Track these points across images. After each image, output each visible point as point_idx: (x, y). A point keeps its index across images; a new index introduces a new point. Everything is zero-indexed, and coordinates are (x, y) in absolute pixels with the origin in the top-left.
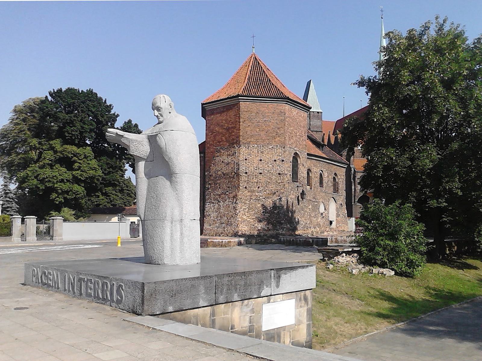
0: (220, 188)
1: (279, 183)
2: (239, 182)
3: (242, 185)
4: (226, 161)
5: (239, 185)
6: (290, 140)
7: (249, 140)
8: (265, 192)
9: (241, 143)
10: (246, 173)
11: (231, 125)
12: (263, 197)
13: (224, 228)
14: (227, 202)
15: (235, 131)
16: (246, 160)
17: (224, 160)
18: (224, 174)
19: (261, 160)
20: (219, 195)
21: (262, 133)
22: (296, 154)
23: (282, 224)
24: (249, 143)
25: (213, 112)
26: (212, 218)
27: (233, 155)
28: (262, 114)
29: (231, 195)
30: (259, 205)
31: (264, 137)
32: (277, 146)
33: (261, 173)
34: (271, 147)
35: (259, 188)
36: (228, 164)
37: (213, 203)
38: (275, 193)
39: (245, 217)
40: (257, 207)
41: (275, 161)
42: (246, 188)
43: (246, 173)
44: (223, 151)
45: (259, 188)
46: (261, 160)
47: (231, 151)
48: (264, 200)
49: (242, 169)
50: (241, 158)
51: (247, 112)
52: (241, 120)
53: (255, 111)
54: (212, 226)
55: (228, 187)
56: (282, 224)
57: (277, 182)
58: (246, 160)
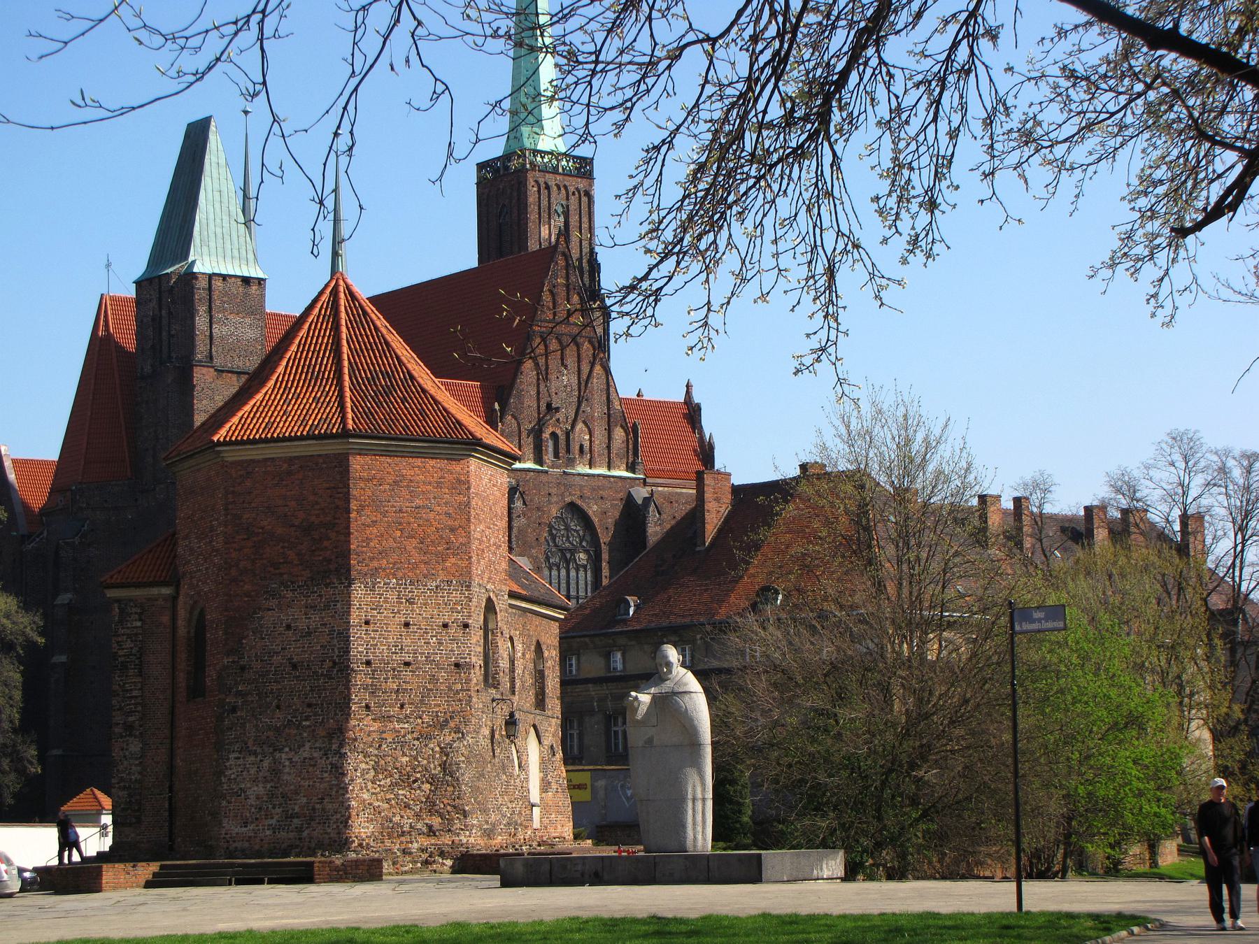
0: (278, 707)
1: (457, 692)
2: (349, 689)
3: (358, 697)
4: (302, 624)
5: (347, 700)
6: (479, 562)
7: (375, 564)
8: (419, 721)
9: (353, 573)
10: (368, 663)
11: (318, 516)
12: (415, 735)
13: (300, 830)
14: (305, 753)
15: (333, 535)
16: (367, 623)
17: (295, 620)
18: (294, 667)
19: (407, 625)
20: (277, 729)
21: (411, 545)
22: (489, 600)
23: (465, 814)
24: (375, 573)
25: (250, 469)
26: (252, 801)
27: (327, 607)
28: (408, 486)
29: (321, 732)
30: (405, 759)
31: (416, 557)
32: (449, 583)
33: (407, 664)
34: (434, 584)
35: (402, 706)
36: (309, 634)
37: (255, 754)
38: (446, 721)
39: (366, 796)
40: (398, 765)
41: (445, 626)
42: (367, 707)
43: (368, 663)
44: (290, 594)
45: (402, 706)
46: (407, 625)
47: (320, 596)
48: (416, 742)
49: (358, 649)
50: (355, 618)
51: (368, 480)
52: (354, 505)
53: (390, 479)
54: (251, 827)
55: (309, 705)
56: (465, 814)
57: (450, 689)
58: (367, 623)
